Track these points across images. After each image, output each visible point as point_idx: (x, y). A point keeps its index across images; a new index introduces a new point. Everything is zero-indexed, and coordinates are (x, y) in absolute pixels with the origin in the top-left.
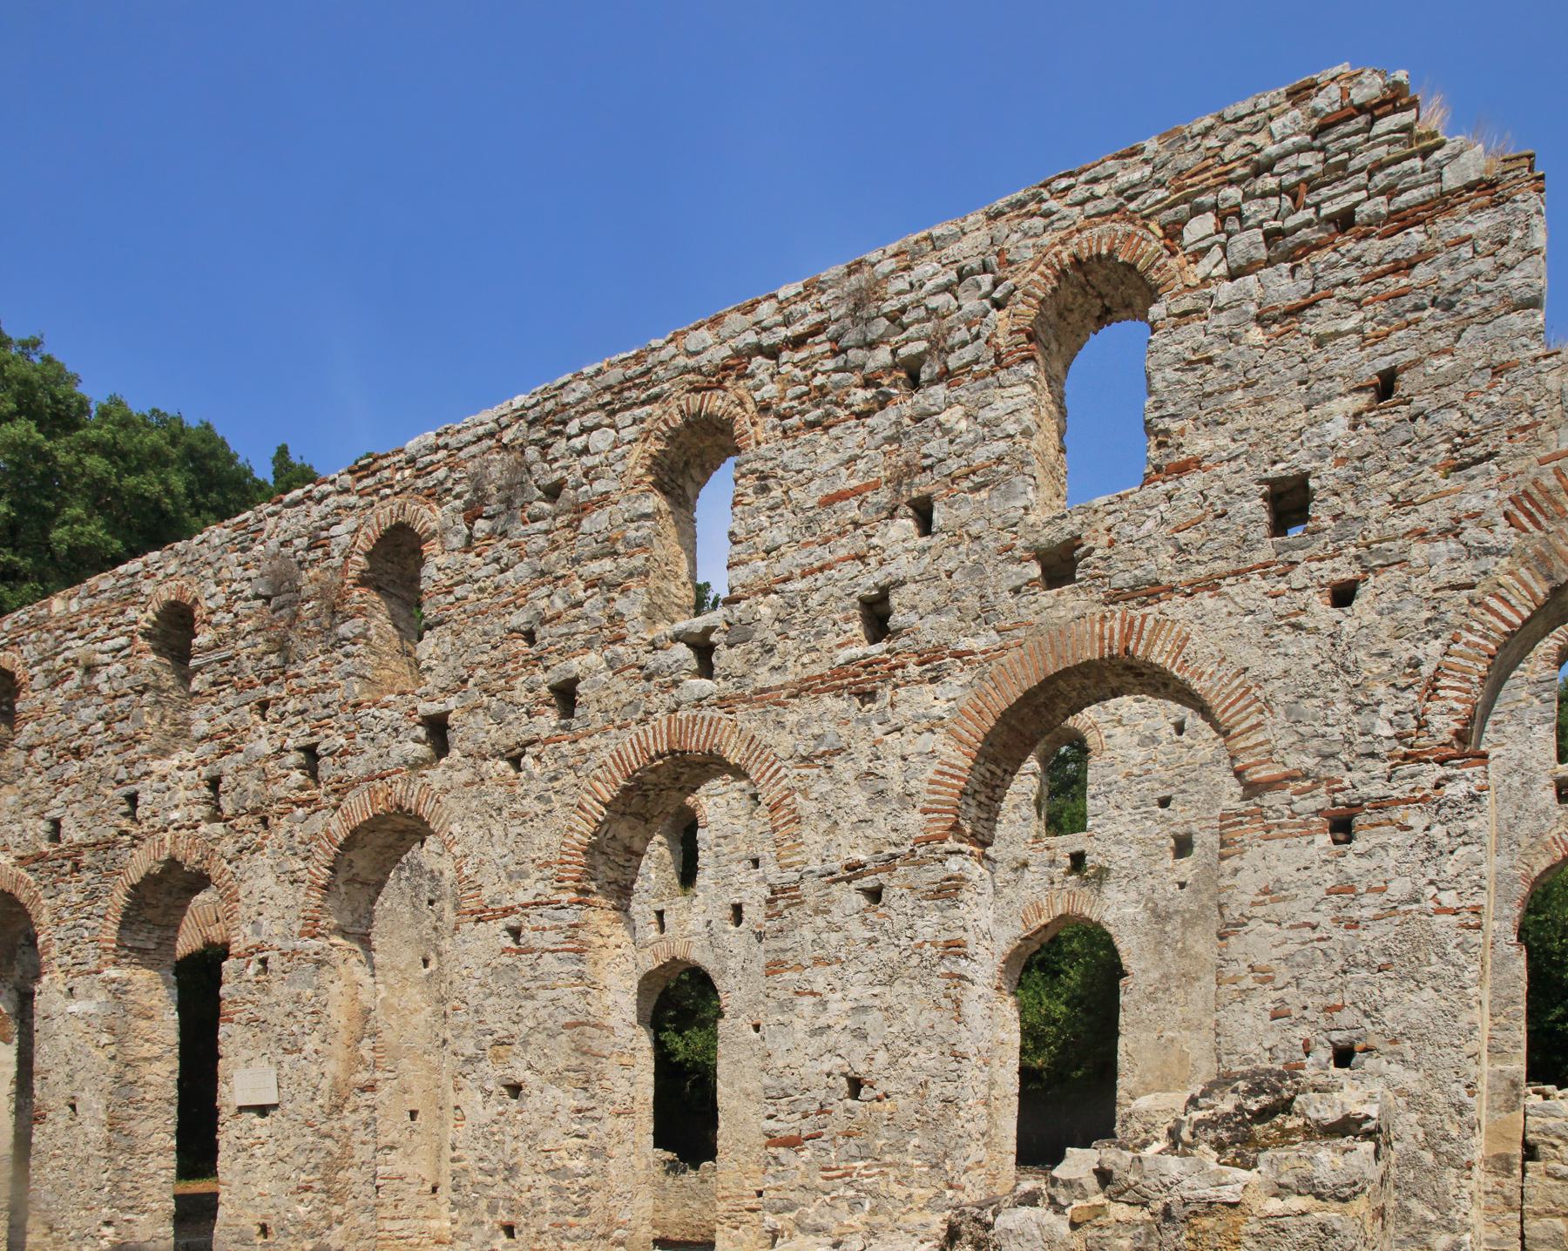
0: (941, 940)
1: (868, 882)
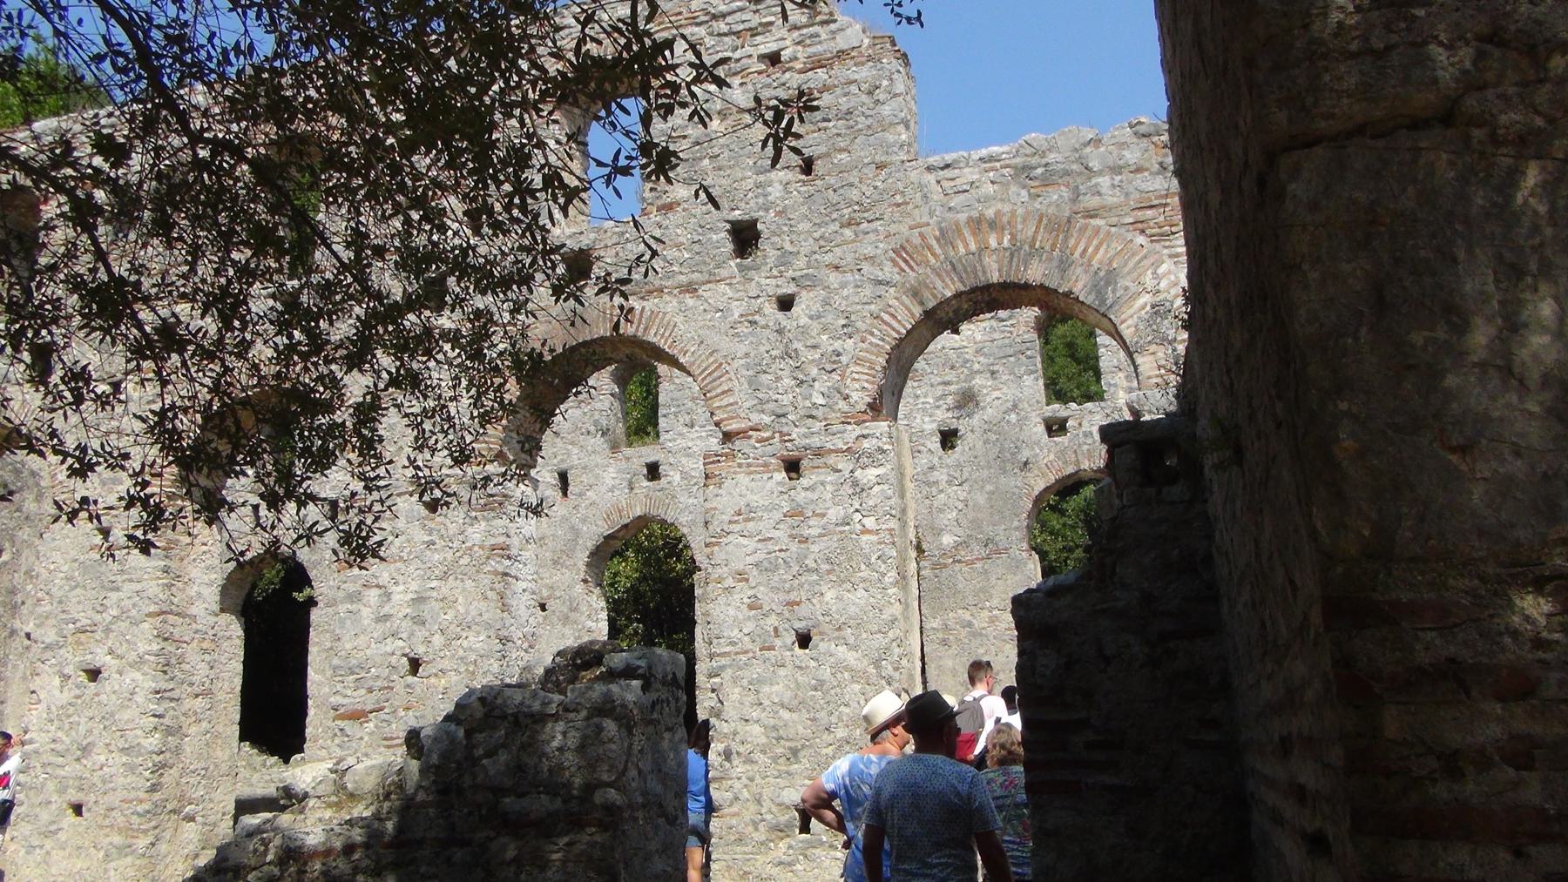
0: (487, 544)
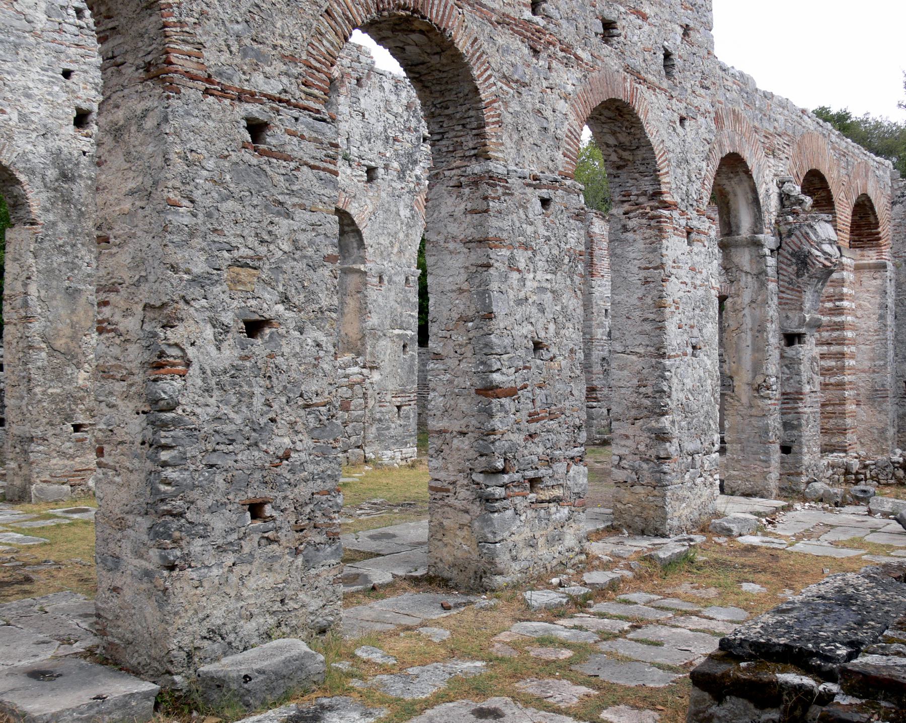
1: (544, 193)
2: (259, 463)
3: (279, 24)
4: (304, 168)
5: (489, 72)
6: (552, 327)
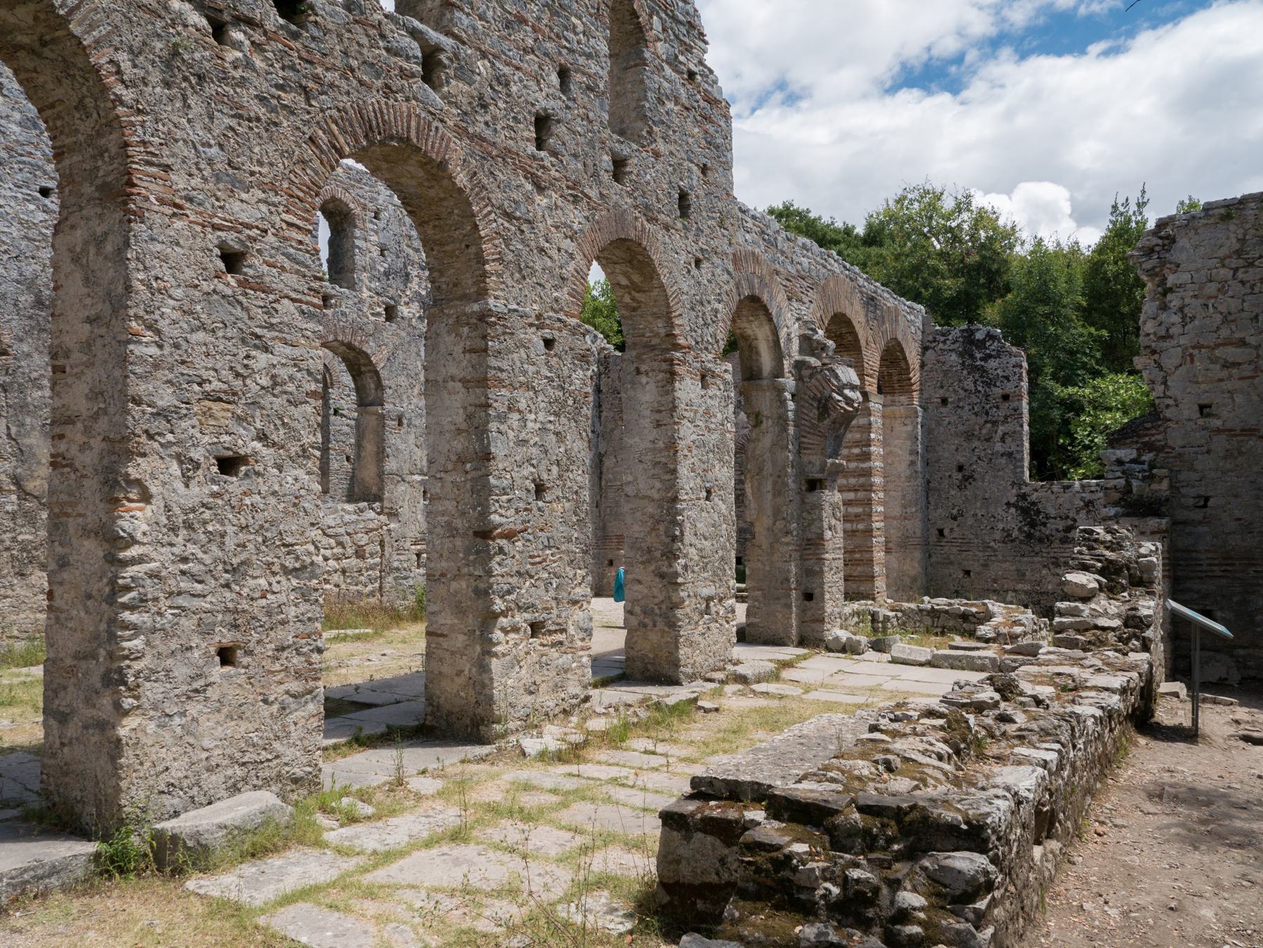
1: (547, 333)
2: (230, 605)
3: (257, 150)
4: (286, 301)
5: (489, 208)
6: (555, 469)
